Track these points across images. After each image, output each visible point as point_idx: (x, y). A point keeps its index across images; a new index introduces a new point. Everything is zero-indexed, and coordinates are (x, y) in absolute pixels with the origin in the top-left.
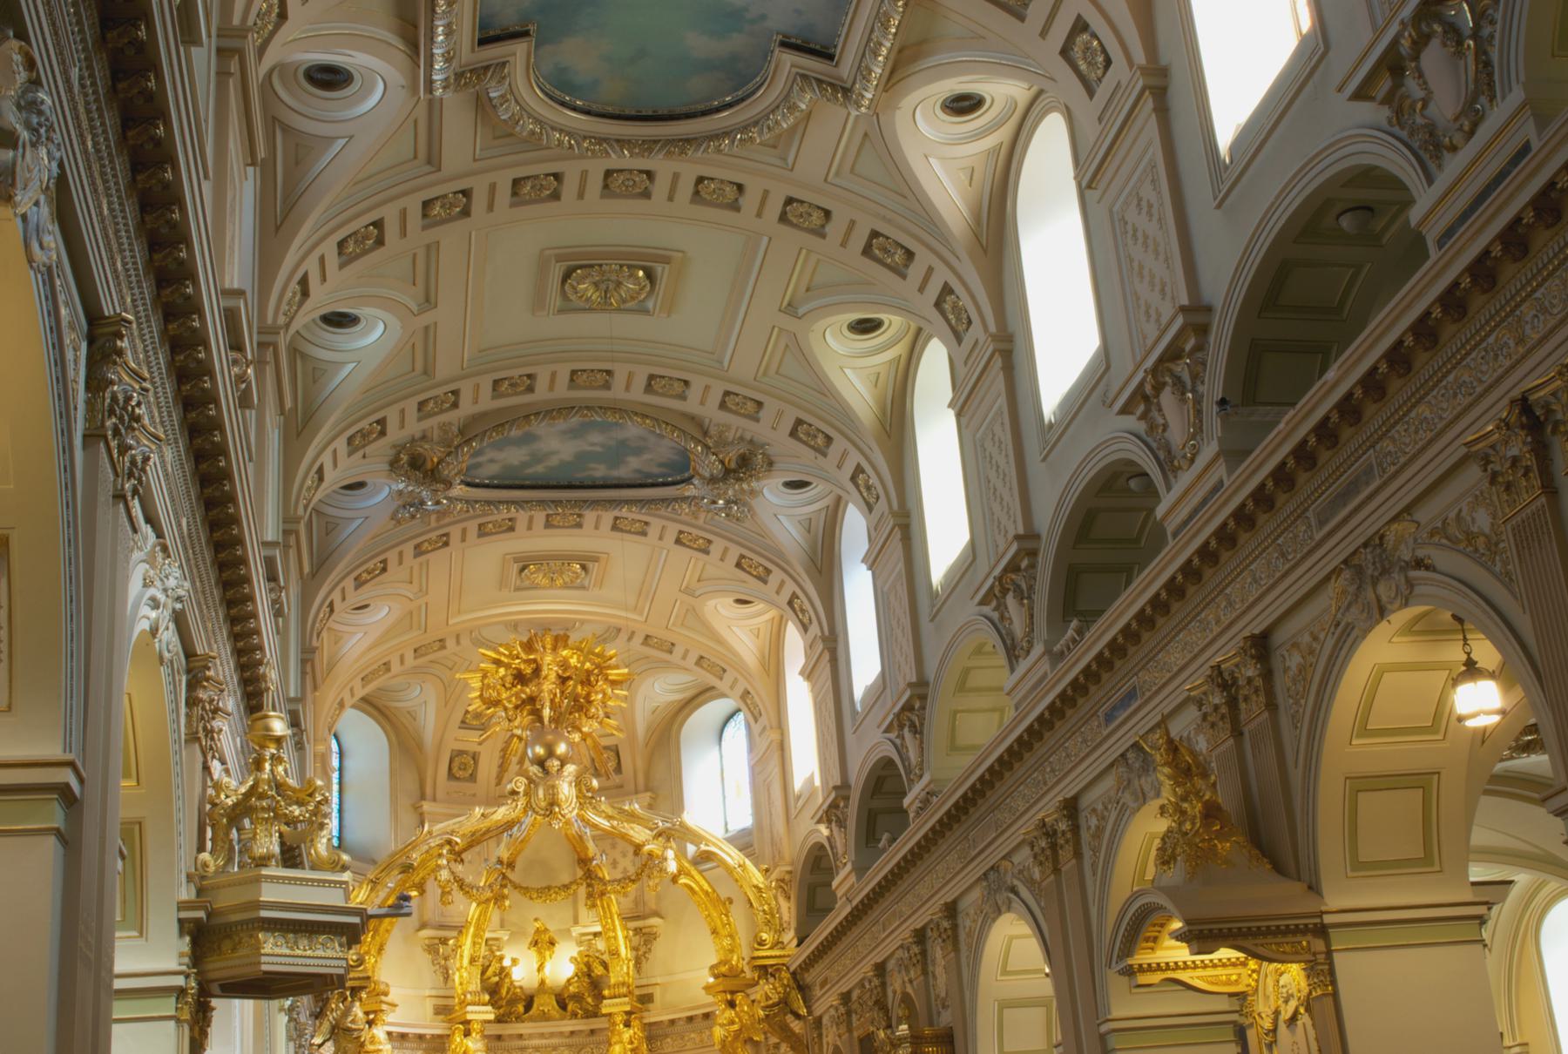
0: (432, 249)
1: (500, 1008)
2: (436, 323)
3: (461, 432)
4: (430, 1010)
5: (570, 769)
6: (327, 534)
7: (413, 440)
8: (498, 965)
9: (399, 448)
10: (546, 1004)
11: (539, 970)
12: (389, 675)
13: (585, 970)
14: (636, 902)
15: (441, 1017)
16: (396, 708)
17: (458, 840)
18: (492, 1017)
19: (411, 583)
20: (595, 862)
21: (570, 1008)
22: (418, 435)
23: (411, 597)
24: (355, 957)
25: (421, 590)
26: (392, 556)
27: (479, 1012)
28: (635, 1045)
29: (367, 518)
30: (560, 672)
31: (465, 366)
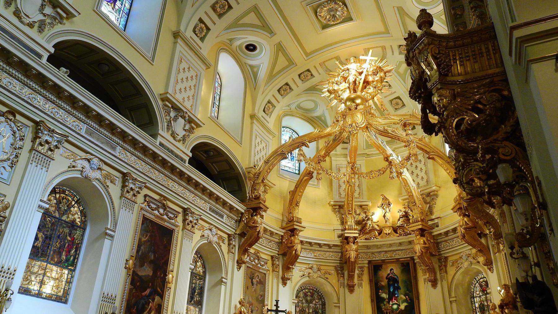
1: (367, 233)
4: (336, 236)
5: (361, 107)
8: (364, 215)
10: (387, 231)
11: (384, 216)
12: (292, 93)
13: (404, 214)
14: (427, 182)
15: (340, 238)
17: (308, 143)
18: (357, 235)
20: (391, 158)
21: (398, 232)
27: (351, 233)
28: (427, 245)
30: (358, 70)
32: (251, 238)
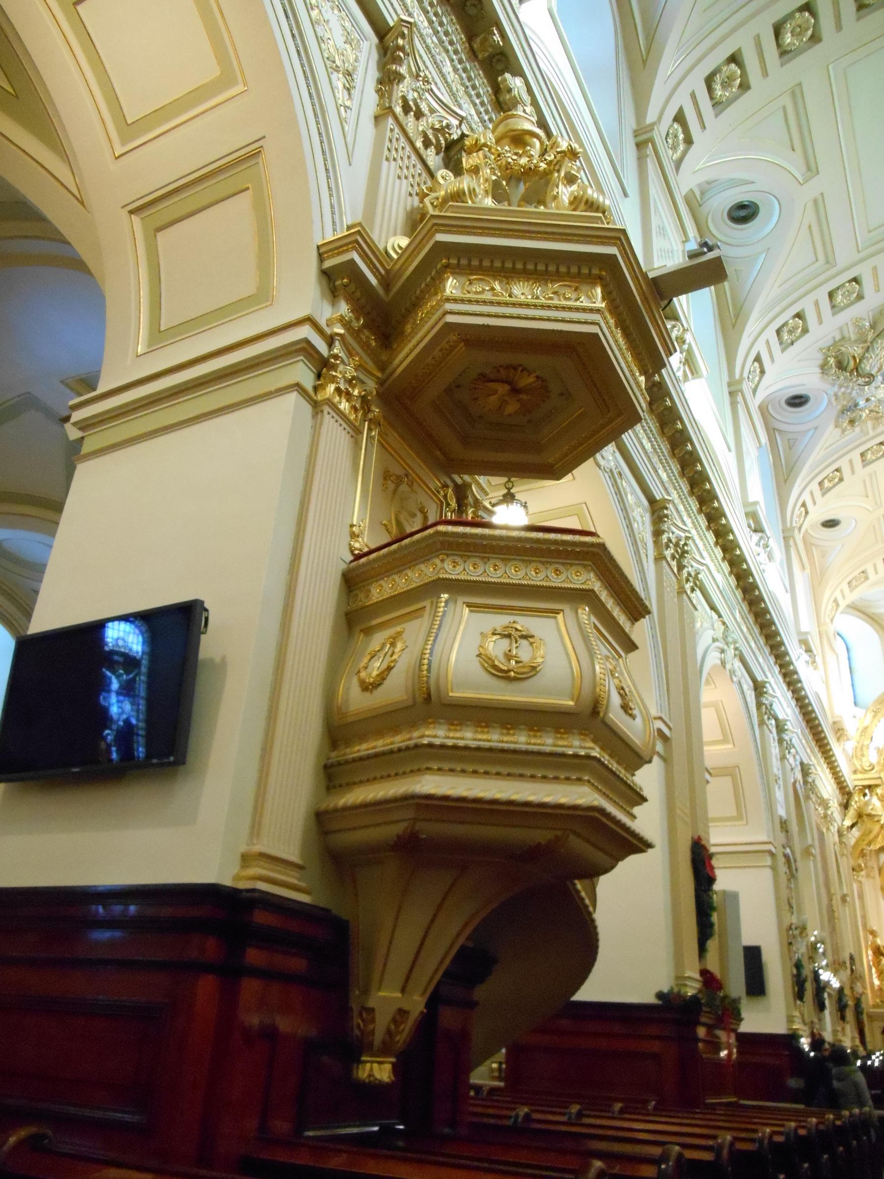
0: (797, 93)
2: (822, 194)
3: (873, 326)
6: (790, 449)
7: (835, 343)
9: (826, 353)
12: (868, 583)
16: (880, 613)
19: (867, 497)
22: (838, 337)
23: (871, 509)
24: (868, 764)
25: (876, 504)
26: (843, 463)
29: (816, 428)
31: (860, 249)
32: (870, 832)
